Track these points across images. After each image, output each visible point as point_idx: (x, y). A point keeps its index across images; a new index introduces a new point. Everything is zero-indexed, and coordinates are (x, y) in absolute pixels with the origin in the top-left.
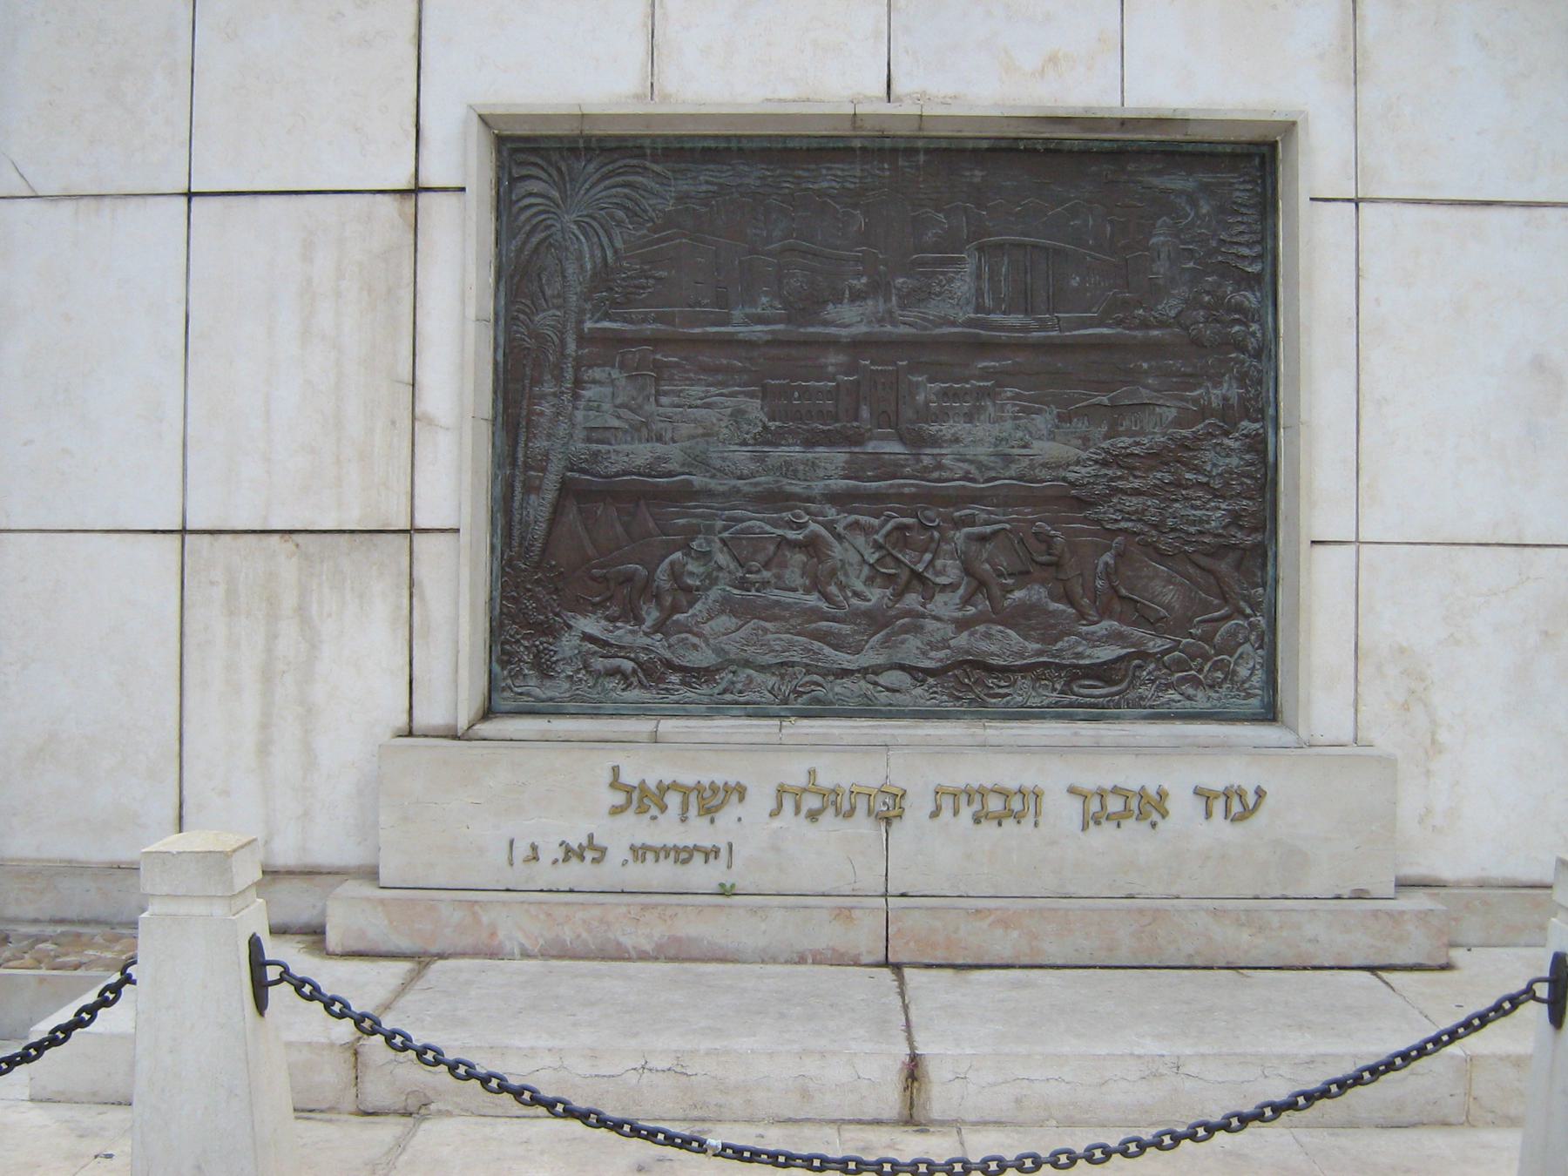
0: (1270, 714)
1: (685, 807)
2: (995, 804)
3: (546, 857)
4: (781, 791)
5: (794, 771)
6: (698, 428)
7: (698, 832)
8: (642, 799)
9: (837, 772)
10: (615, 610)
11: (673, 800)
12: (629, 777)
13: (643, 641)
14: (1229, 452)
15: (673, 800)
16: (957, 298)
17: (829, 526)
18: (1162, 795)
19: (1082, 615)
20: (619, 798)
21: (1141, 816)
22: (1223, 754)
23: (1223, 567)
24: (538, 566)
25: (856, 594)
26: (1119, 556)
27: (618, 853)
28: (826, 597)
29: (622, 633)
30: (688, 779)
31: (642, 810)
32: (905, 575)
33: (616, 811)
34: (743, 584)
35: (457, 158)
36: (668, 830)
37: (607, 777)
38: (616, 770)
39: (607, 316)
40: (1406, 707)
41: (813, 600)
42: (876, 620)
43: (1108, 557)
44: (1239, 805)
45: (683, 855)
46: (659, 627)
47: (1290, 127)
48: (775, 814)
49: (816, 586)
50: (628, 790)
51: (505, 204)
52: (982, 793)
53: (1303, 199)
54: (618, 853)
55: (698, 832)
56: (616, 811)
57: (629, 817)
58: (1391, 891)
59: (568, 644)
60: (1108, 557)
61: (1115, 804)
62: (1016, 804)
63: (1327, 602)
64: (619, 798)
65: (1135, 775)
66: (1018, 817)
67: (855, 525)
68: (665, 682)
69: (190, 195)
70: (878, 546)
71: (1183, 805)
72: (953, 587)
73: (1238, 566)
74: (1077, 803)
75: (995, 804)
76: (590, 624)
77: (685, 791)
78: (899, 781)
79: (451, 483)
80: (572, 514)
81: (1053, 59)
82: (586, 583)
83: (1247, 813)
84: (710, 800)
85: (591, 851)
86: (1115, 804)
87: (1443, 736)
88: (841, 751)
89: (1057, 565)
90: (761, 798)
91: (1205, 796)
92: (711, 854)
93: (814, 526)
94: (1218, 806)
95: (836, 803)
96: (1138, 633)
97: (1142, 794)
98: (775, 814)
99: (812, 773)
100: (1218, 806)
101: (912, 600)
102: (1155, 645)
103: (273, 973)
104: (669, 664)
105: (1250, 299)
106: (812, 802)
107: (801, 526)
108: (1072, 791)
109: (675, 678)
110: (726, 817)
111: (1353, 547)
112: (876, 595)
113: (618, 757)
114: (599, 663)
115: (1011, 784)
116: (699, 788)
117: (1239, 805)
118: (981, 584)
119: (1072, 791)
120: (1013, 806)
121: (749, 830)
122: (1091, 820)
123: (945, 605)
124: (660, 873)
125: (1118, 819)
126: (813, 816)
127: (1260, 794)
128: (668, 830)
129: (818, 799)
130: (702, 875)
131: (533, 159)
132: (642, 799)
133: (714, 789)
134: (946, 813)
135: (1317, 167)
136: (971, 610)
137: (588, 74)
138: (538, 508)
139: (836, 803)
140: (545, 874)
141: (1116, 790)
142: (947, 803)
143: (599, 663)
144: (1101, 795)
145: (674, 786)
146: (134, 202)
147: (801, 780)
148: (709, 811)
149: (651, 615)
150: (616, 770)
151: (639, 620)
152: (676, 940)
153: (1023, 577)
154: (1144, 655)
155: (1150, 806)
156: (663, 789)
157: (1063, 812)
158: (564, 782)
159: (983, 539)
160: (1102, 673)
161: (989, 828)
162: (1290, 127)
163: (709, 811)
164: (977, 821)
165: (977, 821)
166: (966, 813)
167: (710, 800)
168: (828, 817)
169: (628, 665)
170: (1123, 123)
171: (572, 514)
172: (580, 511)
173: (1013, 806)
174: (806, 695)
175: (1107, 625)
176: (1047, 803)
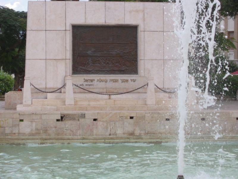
0: (137, 74)
1: (90, 81)
4: (98, 80)
7: (91, 83)
8: (86, 81)
9: (102, 78)
11: (89, 81)
12: (85, 79)
13: (85, 68)
14: (134, 52)
15: (89, 81)
18: (128, 80)
19: (122, 66)
20: (85, 81)
21: (126, 82)
22: (133, 77)
23: (133, 62)
26: (125, 61)
27: (84, 85)
28: (101, 65)
29: (83, 68)
30: (90, 79)
31: (86, 81)
32: (107, 63)
33: (84, 82)
34: (93, 64)
35: (69, 28)
36: (89, 83)
37: (83, 79)
38: (84, 78)
40: (148, 73)
41: (99, 65)
43: (124, 61)
44: (134, 81)
45: (90, 85)
46: (86, 67)
47: (138, 25)
48: (97, 82)
49: (99, 64)
50: (85, 80)
51: (73, 32)
52: (113, 80)
53: (139, 30)
55: (91, 83)
56: (84, 82)
57: (85, 82)
59: (79, 69)
60: (124, 61)
62: (116, 81)
63: (142, 65)
64: (85, 81)
66: (116, 82)
67: (103, 59)
69: (46, 30)
70: (104, 60)
71: (130, 81)
72: (110, 64)
74: (121, 81)
75: (115, 81)
76: (81, 67)
78: (107, 79)
79: (69, 55)
83: (135, 82)
85: (83, 85)
86: (124, 81)
89: (119, 62)
91: (131, 80)
92: (92, 85)
93: (99, 59)
94: (132, 81)
96: (126, 67)
97: (126, 80)
98: (97, 82)
99: (100, 78)
100: (132, 81)
101: (107, 65)
102: (128, 68)
104: (87, 70)
106: (100, 81)
107: (98, 59)
108: (121, 80)
109: (88, 71)
110: (93, 82)
111: (143, 61)
112: (104, 65)
113: (84, 77)
114: (81, 70)
115: (116, 79)
116: (91, 80)
117: (134, 81)
118: (113, 64)
119: (121, 80)
120: (116, 81)
121: (95, 83)
122: (122, 82)
123: (110, 65)
125: (124, 82)
126: (100, 82)
127: (136, 80)
128: (89, 83)
129: (100, 81)
131: (76, 28)
132: (86, 81)
133: (92, 80)
134: (111, 82)
135: (140, 29)
136: (112, 66)
137: (80, 21)
141: (124, 80)
142: (111, 81)
143: (81, 70)
144: (123, 80)
145: (89, 80)
146: (41, 31)
147: (99, 79)
148: (92, 81)
149: (86, 66)
150: (84, 78)
151: (85, 67)
153: (117, 63)
154: (127, 69)
155: (127, 81)
156: (88, 80)
157: (120, 81)
158: (80, 79)
159: (113, 60)
160: (123, 71)
161: (114, 83)
162: (138, 25)
163: (92, 81)
164: (113, 82)
165: (113, 82)
167: (92, 81)
168: (101, 82)
169: (84, 71)
170: (125, 25)
173: (116, 81)
175: (124, 67)
176: (119, 81)
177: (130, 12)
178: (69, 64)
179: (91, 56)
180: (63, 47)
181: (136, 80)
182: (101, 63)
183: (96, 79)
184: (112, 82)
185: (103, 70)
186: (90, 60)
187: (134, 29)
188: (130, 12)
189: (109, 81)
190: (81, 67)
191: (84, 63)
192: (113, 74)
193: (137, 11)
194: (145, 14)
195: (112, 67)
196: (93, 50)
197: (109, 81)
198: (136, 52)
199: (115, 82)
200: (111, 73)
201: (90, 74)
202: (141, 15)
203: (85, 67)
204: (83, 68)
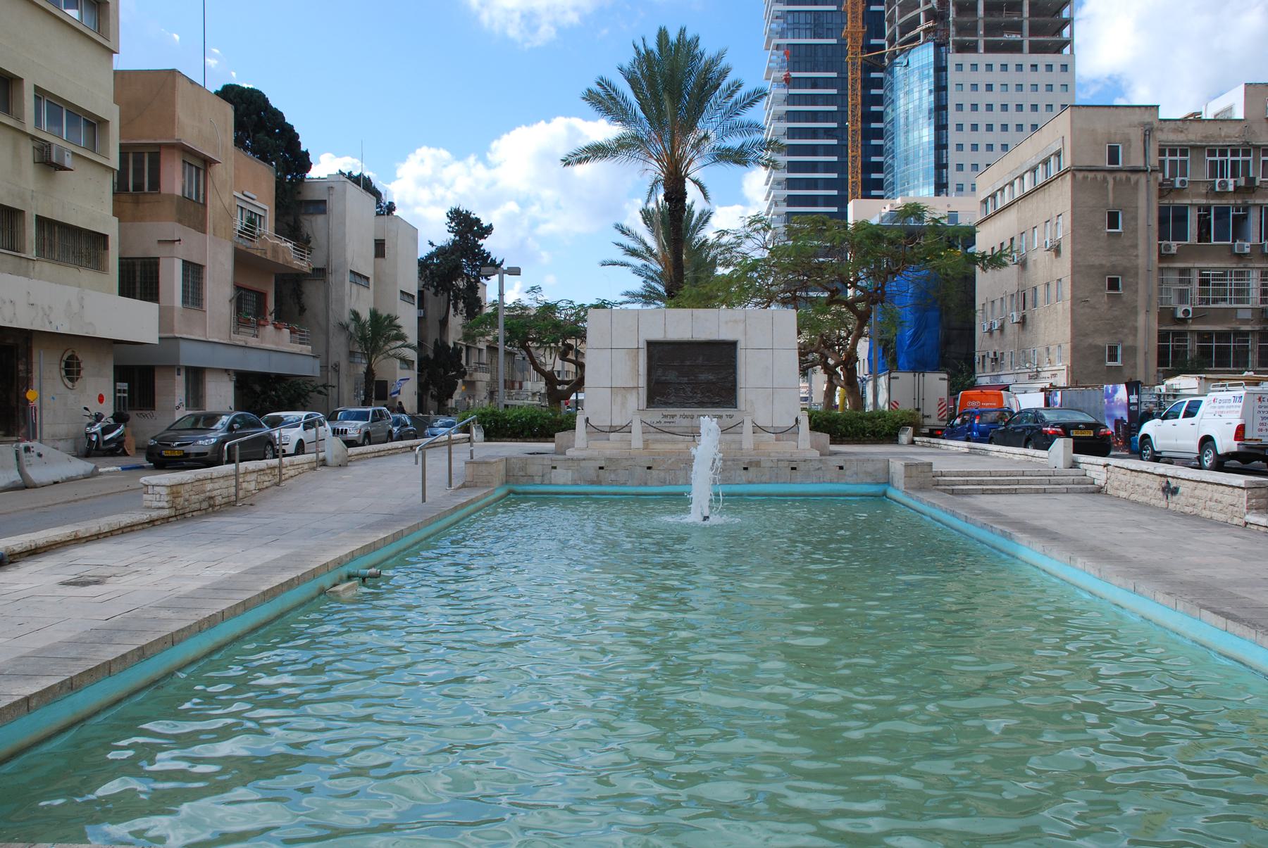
6: (672, 376)
8: (665, 416)
16: (700, 361)
35: (643, 345)
44: (731, 417)
63: (742, 395)
68: (667, 404)
79: (643, 382)
82: (658, 393)
84: (673, 416)
88: (687, 411)
95: (686, 417)
117: (731, 417)
121: (677, 419)
132: (665, 416)
137: (658, 336)
139: (686, 417)
158: (656, 415)
167: (673, 416)
174: (683, 405)
178: (643, 393)
180: (633, 372)
187: (732, 345)
193: (736, 321)
202: (741, 326)
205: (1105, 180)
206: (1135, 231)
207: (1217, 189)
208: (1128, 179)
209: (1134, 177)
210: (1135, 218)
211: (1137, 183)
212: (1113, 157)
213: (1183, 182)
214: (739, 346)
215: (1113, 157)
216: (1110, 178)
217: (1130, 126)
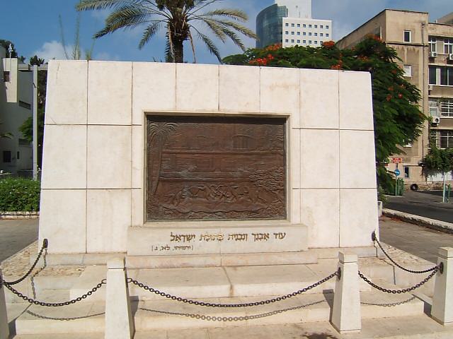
2: (239, 237)
3: (159, 249)
4: (202, 236)
5: (203, 232)
7: (187, 244)
8: (177, 238)
10: (169, 202)
14: (278, 173)
17: (208, 187)
20: (173, 238)
23: (277, 192)
24: (155, 194)
25: (213, 199)
27: (172, 248)
29: (171, 206)
33: (172, 240)
34: (192, 197)
35: (140, 119)
36: (181, 243)
39: (167, 148)
42: (217, 203)
44: (282, 236)
45: (184, 248)
49: (205, 197)
51: (148, 130)
54: (172, 248)
56: (172, 240)
58: (307, 250)
61: (260, 236)
63: (296, 200)
64: (173, 238)
65: (263, 231)
73: (279, 192)
76: (165, 205)
77: (184, 236)
79: (139, 179)
80: (160, 184)
81: (248, 103)
84: (189, 238)
86: (260, 236)
87: (315, 222)
90: (198, 237)
103: (129, 280)
105: (281, 145)
112: (217, 199)
113: (173, 231)
117: (282, 236)
121: (195, 242)
123: (229, 201)
124: (179, 251)
126: (207, 240)
127: (285, 234)
128: (181, 243)
130: (187, 251)
131: (153, 118)
132: (177, 238)
134: (231, 239)
138: (154, 184)
140: (158, 252)
148: (188, 240)
152: (184, 264)
155: (266, 236)
157: (251, 238)
159: (235, 188)
160: (256, 212)
163: (188, 240)
166: (234, 239)
167: (189, 238)
169: (171, 212)
171: (160, 184)
172: (163, 185)
173: (242, 237)
177: (270, 87)
179: (187, 181)
181: (285, 234)
182: (209, 195)
183: (198, 233)
184: (233, 241)
185: (215, 211)
186: (185, 190)
187: (280, 121)
188: (272, 88)
189: (226, 238)
190: (165, 205)
191: (171, 196)
192: (235, 218)
193: (286, 87)
194: (302, 92)
195: (233, 203)
196: (192, 167)
197: (226, 238)
198: (284, 172)
199: (240, 239)
200: (232, 218)
201: (184, 219)
203: (173, 204)
204: (171, 206)
205: (403, 49)
206: (417, 76)
207: (451, 59)
208: (414, 50)
209: (417, 48)
210: (418, 70)
211: (418, 51)
212: (407, 38)
213: (435, 54)
214: (293, 123)
215: (407, 38)
216: (405, 48)
217: (415, 22)
